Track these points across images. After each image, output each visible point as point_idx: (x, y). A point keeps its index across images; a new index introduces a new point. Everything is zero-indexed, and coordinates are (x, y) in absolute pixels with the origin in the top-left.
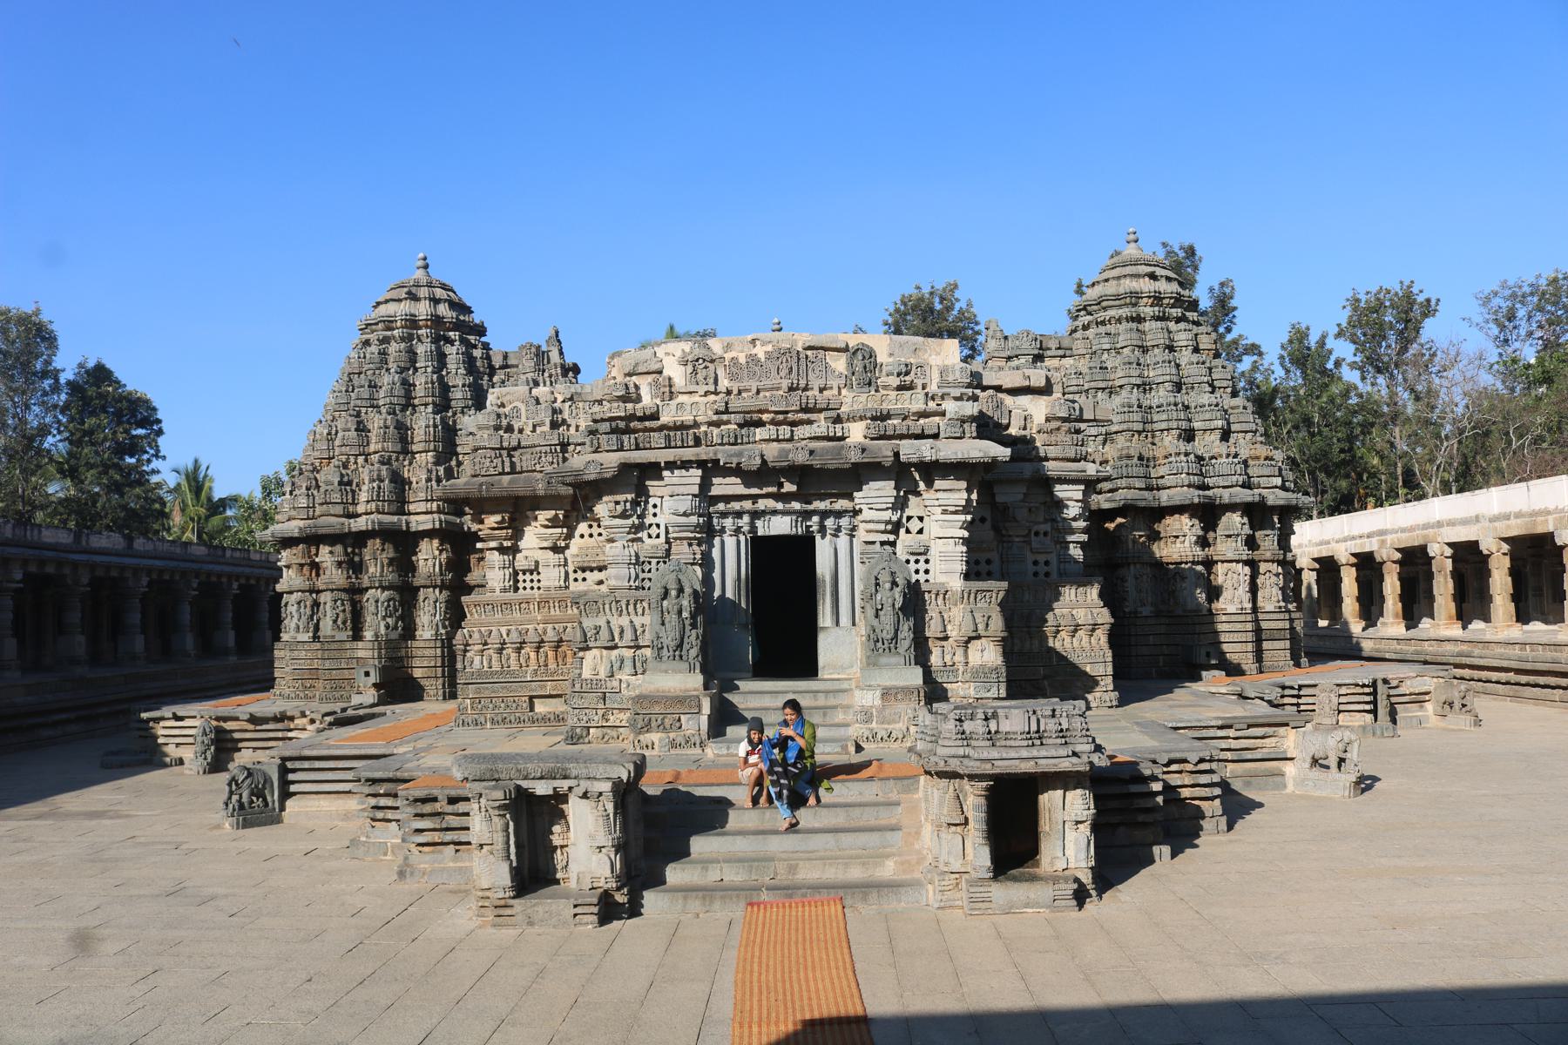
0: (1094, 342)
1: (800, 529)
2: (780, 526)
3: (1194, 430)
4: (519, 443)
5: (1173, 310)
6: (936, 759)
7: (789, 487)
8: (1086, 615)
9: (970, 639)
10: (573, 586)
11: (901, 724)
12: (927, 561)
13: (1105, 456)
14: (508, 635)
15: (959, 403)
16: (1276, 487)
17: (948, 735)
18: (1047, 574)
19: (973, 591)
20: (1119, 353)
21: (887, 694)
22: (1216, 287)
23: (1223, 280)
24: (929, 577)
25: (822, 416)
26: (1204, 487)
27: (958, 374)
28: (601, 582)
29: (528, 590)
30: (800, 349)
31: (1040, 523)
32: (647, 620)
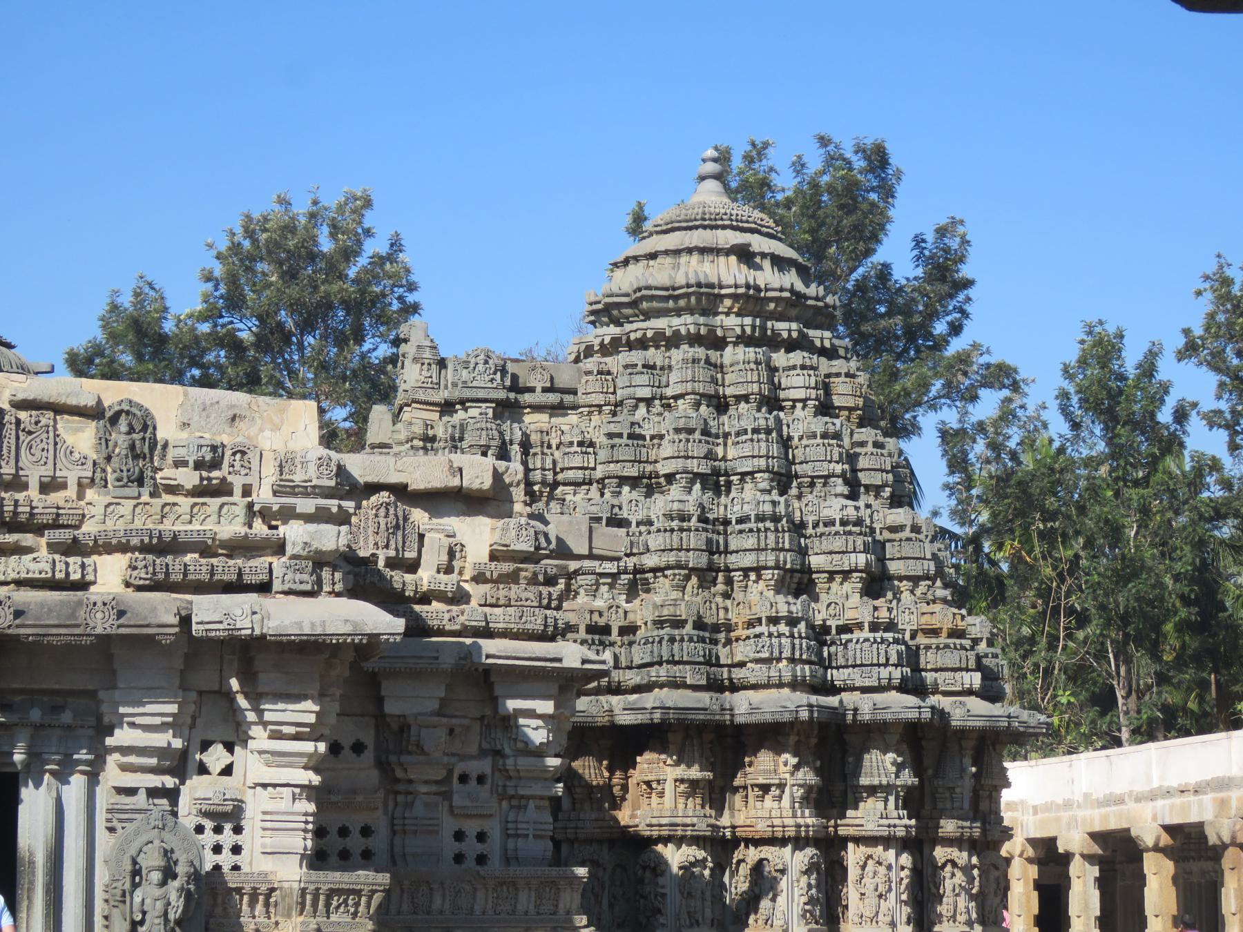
0: (619, 383)
3: (810, 571)
5: (782, 326)
12: (238, 830)
13: (631, 617)
15: (312, 527)
16: (970, 692)
18: (481, 859)
19: (325, 887)
20: (669, 406)
22: (930, 237)
23: (943, 221)
25: (43, 541)
26: (830, 689)
27: (312, 471)
31: (472, 757)
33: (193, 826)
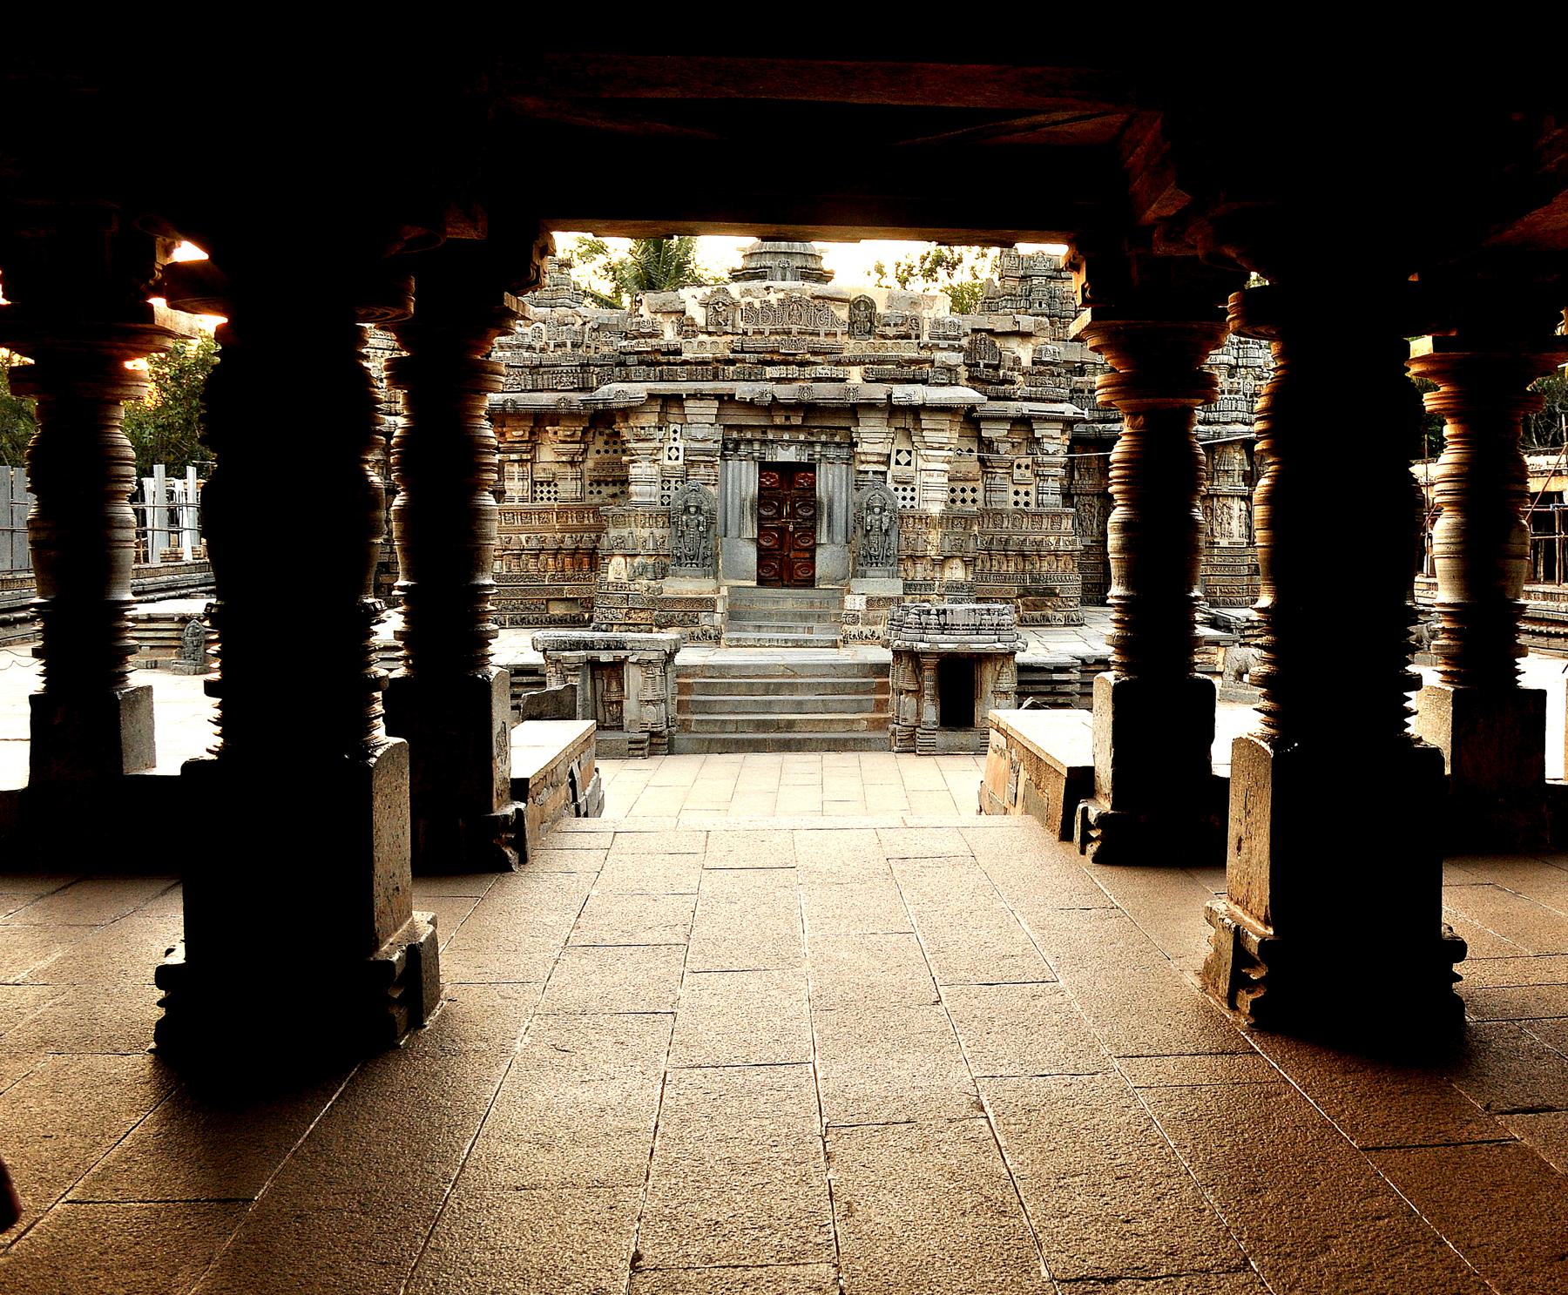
1: (803, 458)
2: (787, 455)
4: (541, 362)
6: (899, 642)
7: (797, 420)
8: (1058, 542)
9: (947, 558)
10: (587, 495)
11: (882, 626)
12: (913, 490)
14: (527, 541)
15: (945, 353)
17: (909, 626)
21: (870, 602)
24: (915, 503)
28: (614, 496)
29: (545, 502)
30: (809, 299)
32: (665, 532)
33: (892, 489)
